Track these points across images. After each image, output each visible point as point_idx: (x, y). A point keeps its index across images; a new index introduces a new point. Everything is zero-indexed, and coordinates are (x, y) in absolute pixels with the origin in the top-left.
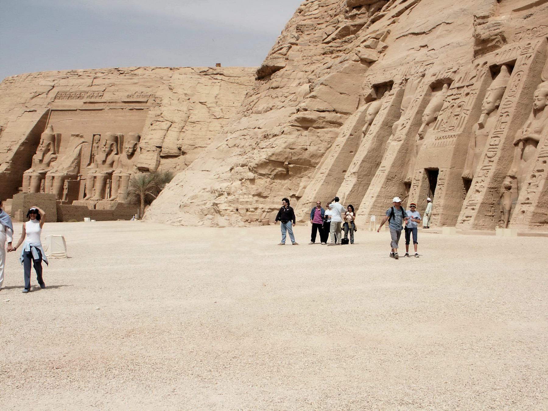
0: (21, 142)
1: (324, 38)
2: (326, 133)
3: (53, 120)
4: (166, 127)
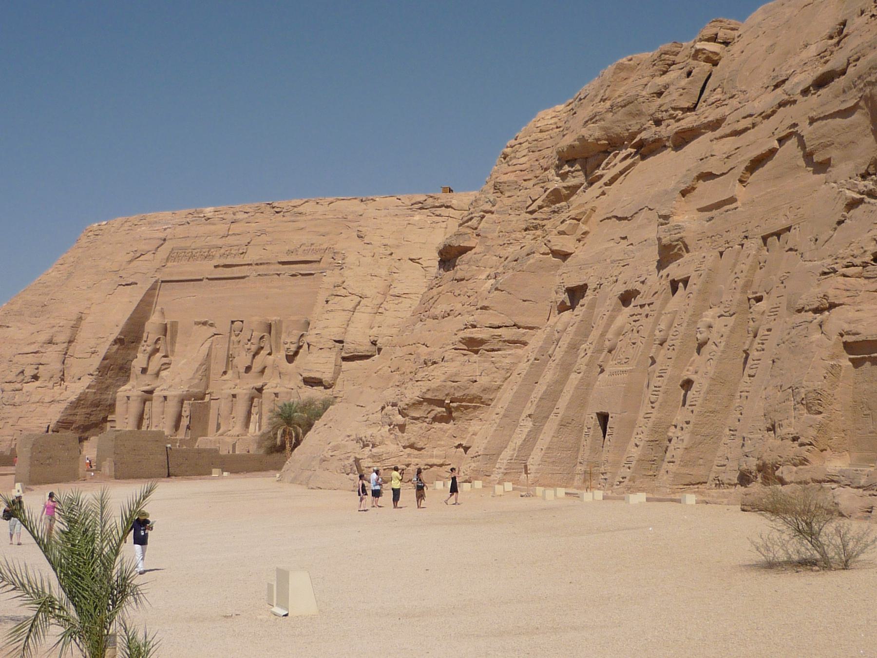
0: (112, 338)
1: (528, 204)
2: (506, 357)
3: (164, 298)
4: (350, 306)
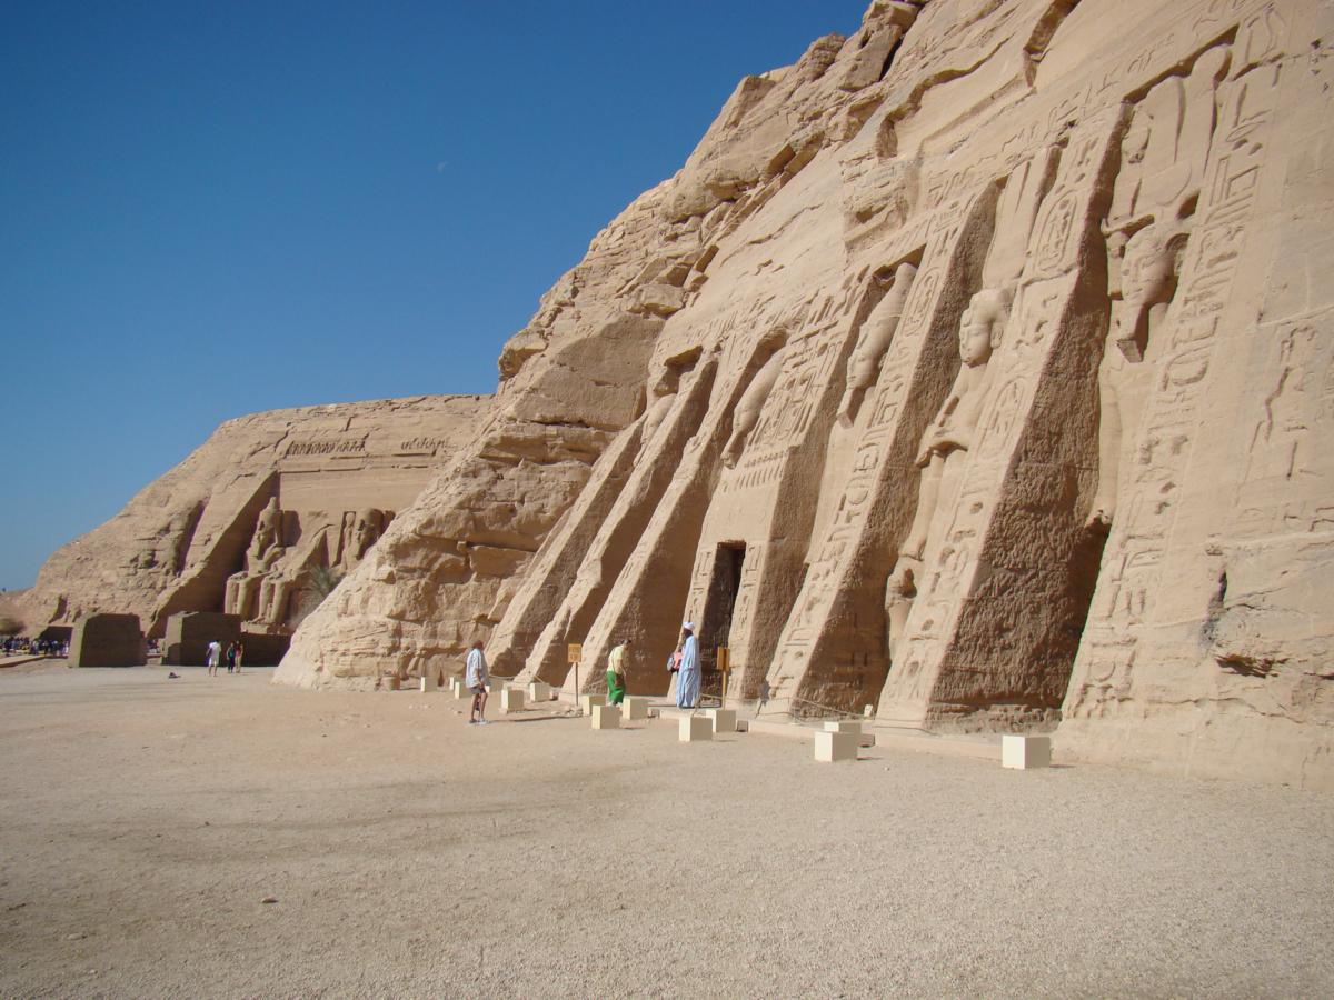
0: (227, 526)
2: (561, 473)
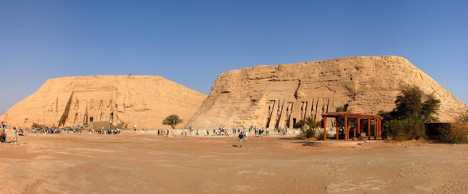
3: (74, 95)
